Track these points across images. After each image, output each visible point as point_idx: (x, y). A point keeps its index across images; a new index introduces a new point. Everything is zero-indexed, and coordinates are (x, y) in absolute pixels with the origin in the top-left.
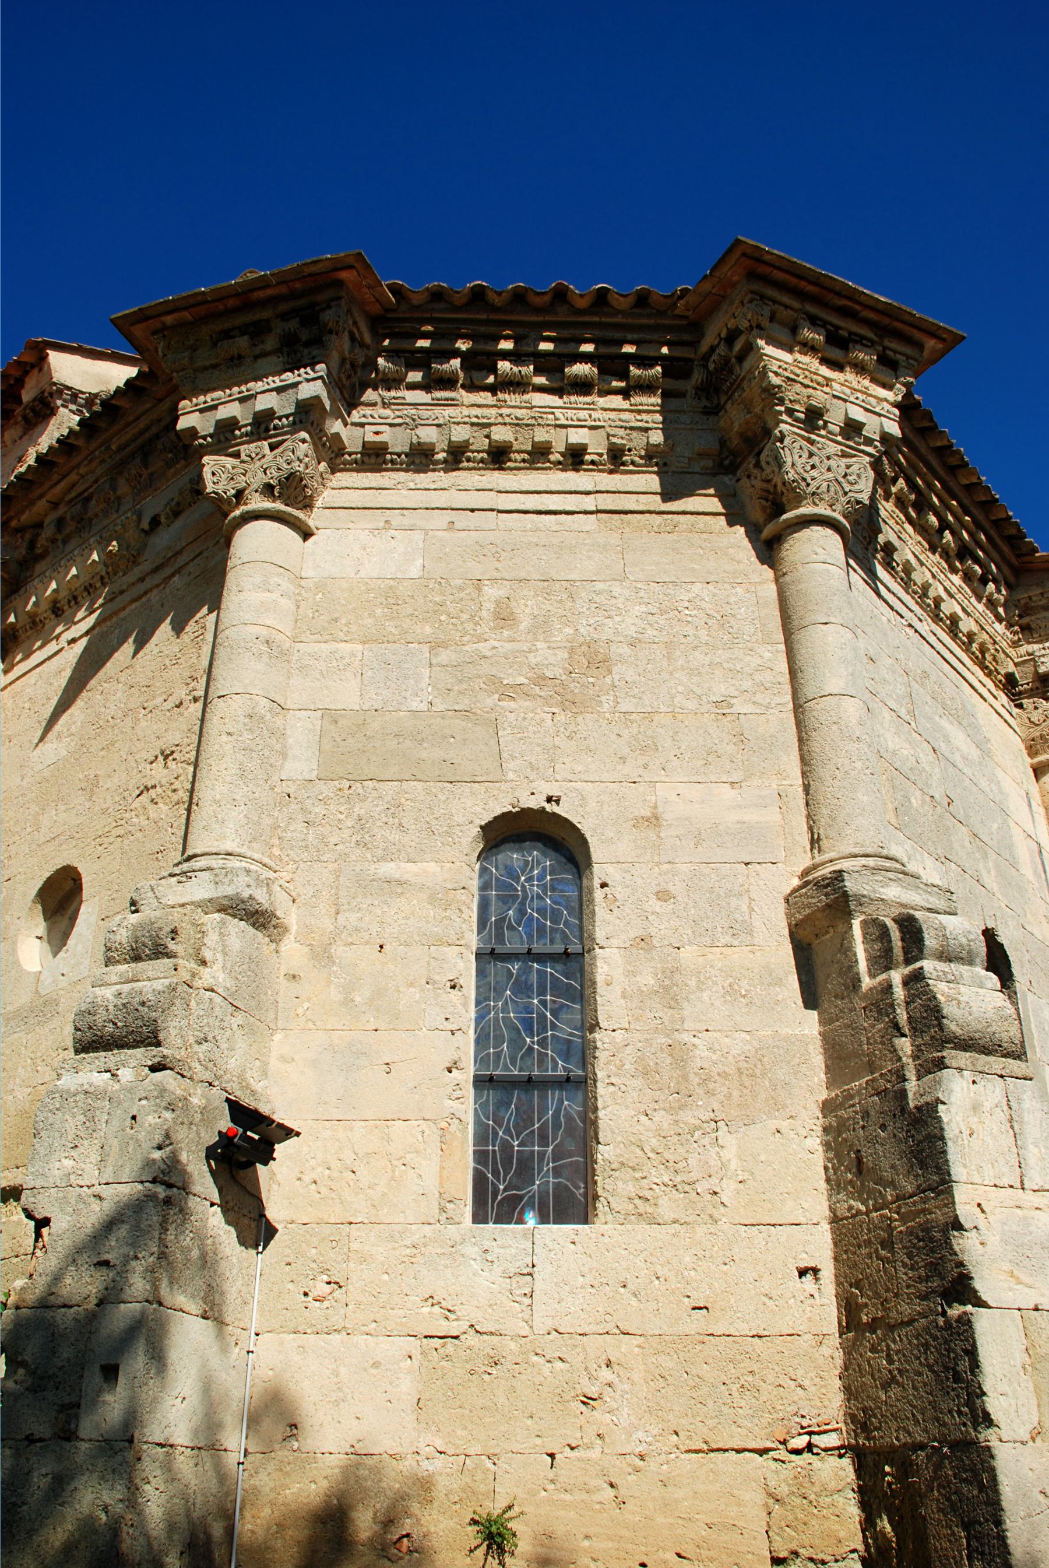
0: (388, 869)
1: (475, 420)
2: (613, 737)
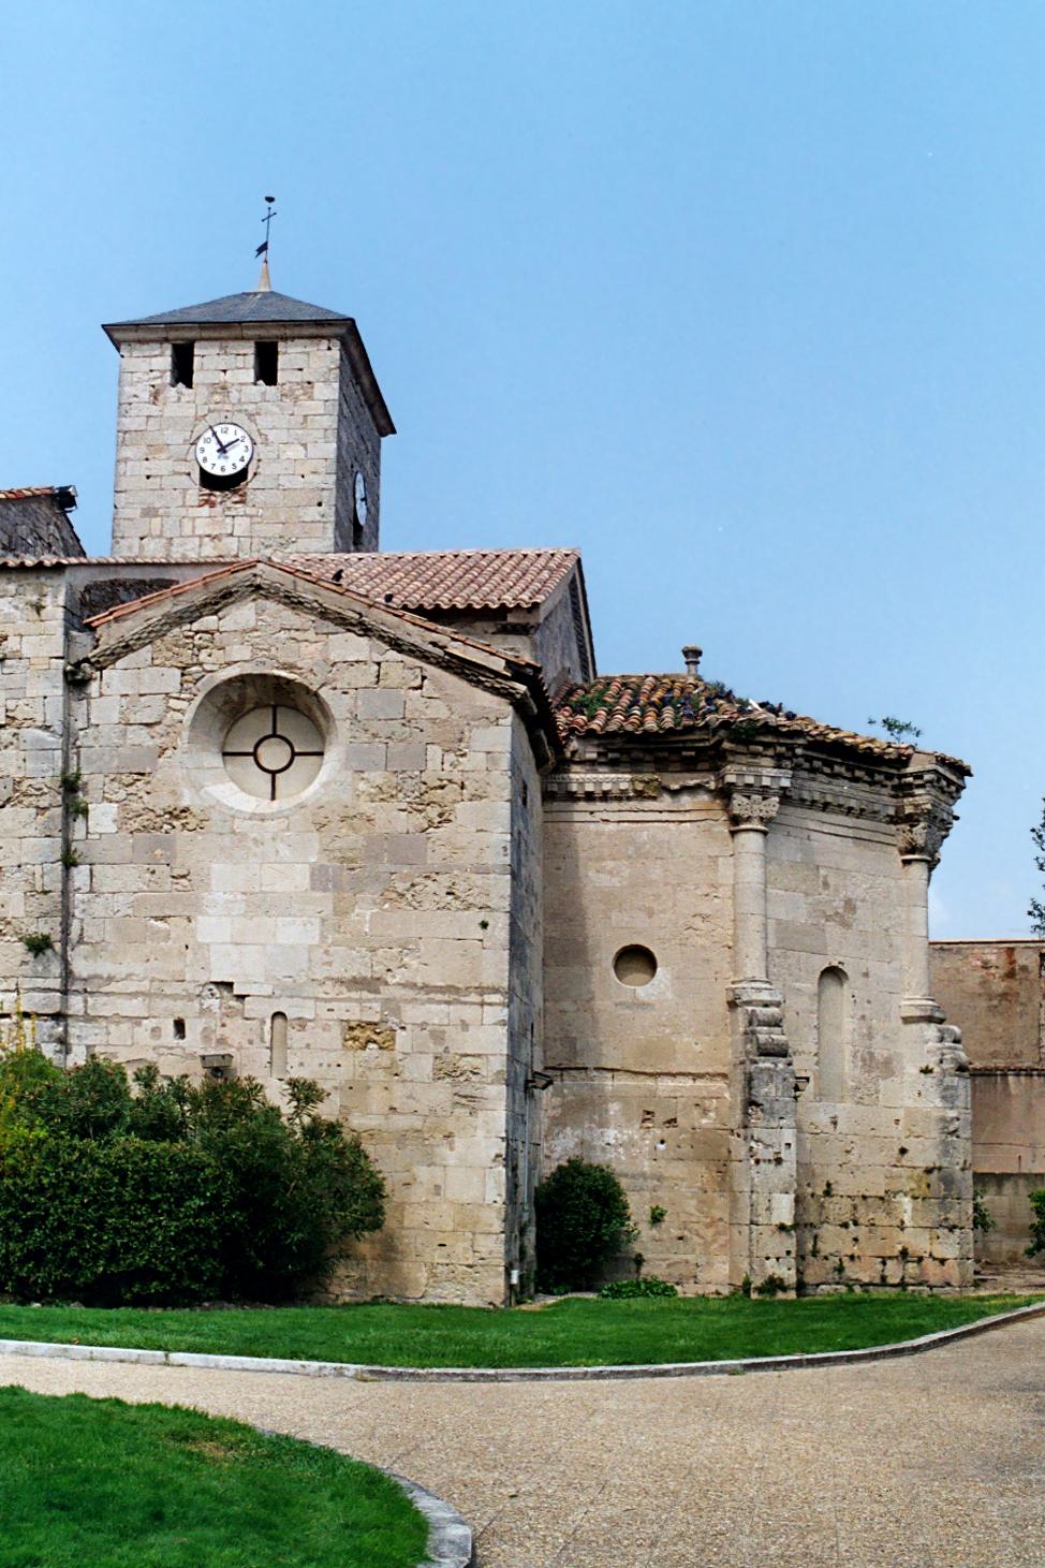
0: (797, 985)
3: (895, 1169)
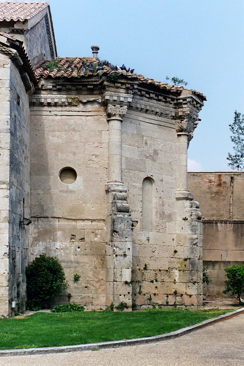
0: (134, 184)
1: (145, 104)
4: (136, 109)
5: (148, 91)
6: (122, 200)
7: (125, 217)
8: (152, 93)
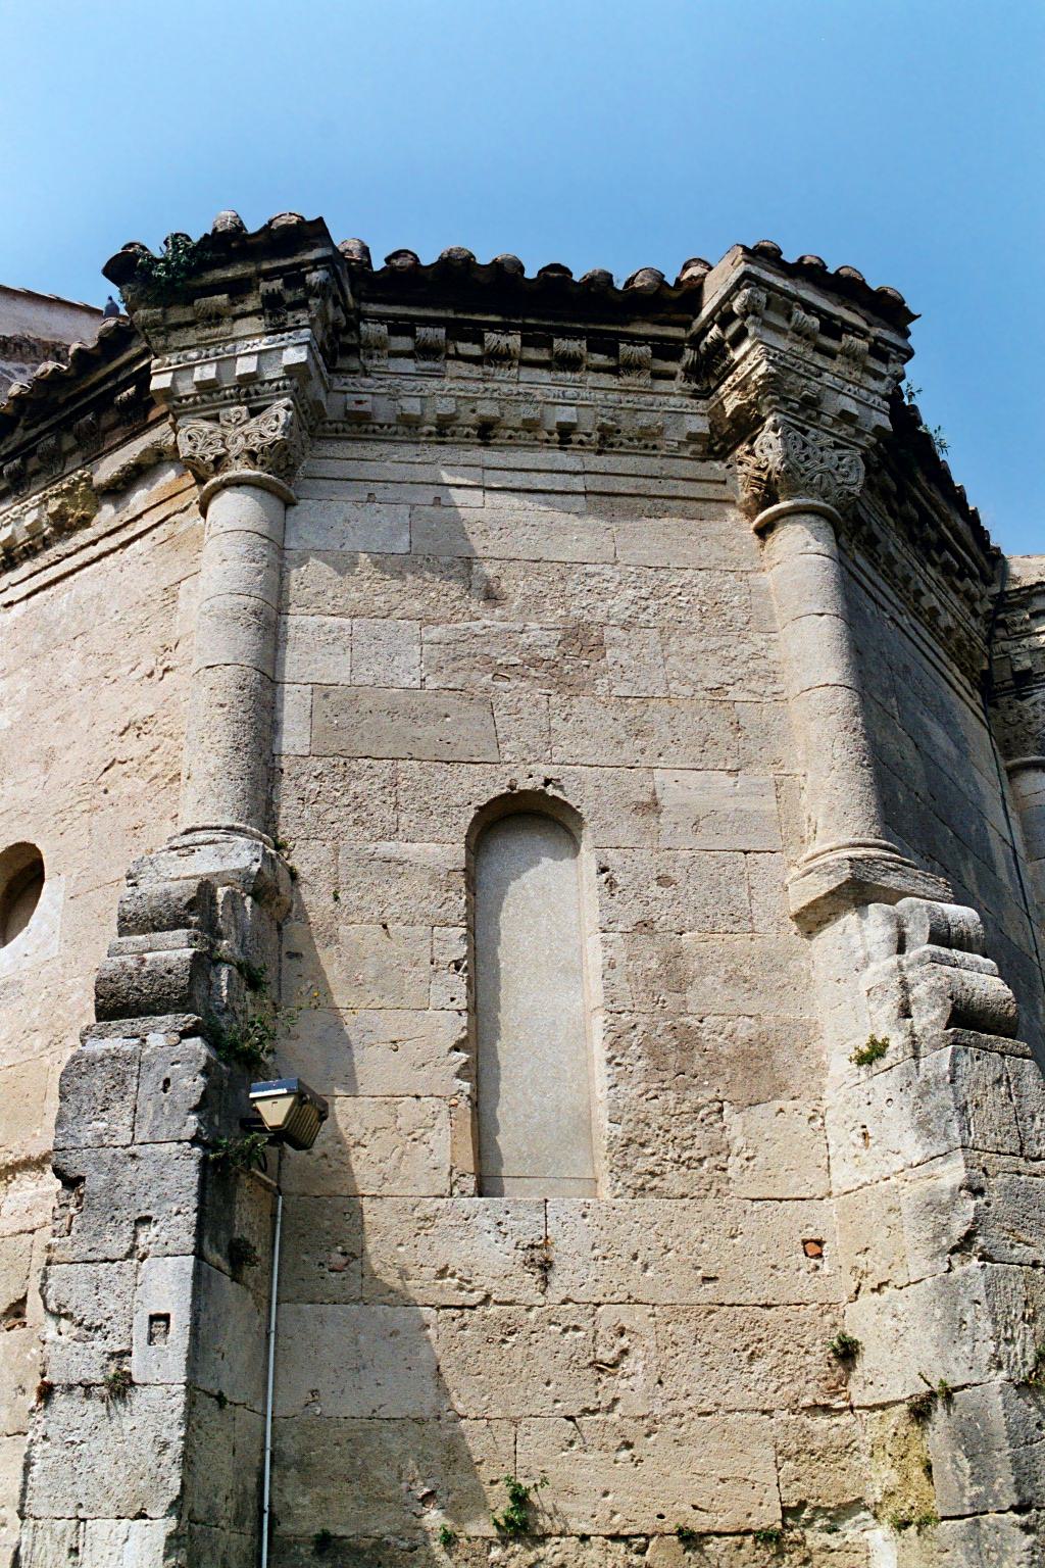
0: (386, 848)
1: (462, 394)
2: (610, 722)
3: (822, 1422)
4: (401, 429)
5: (460, 316)
6: (156, 929)
7: (148, 1051)
8: (492, 327)
